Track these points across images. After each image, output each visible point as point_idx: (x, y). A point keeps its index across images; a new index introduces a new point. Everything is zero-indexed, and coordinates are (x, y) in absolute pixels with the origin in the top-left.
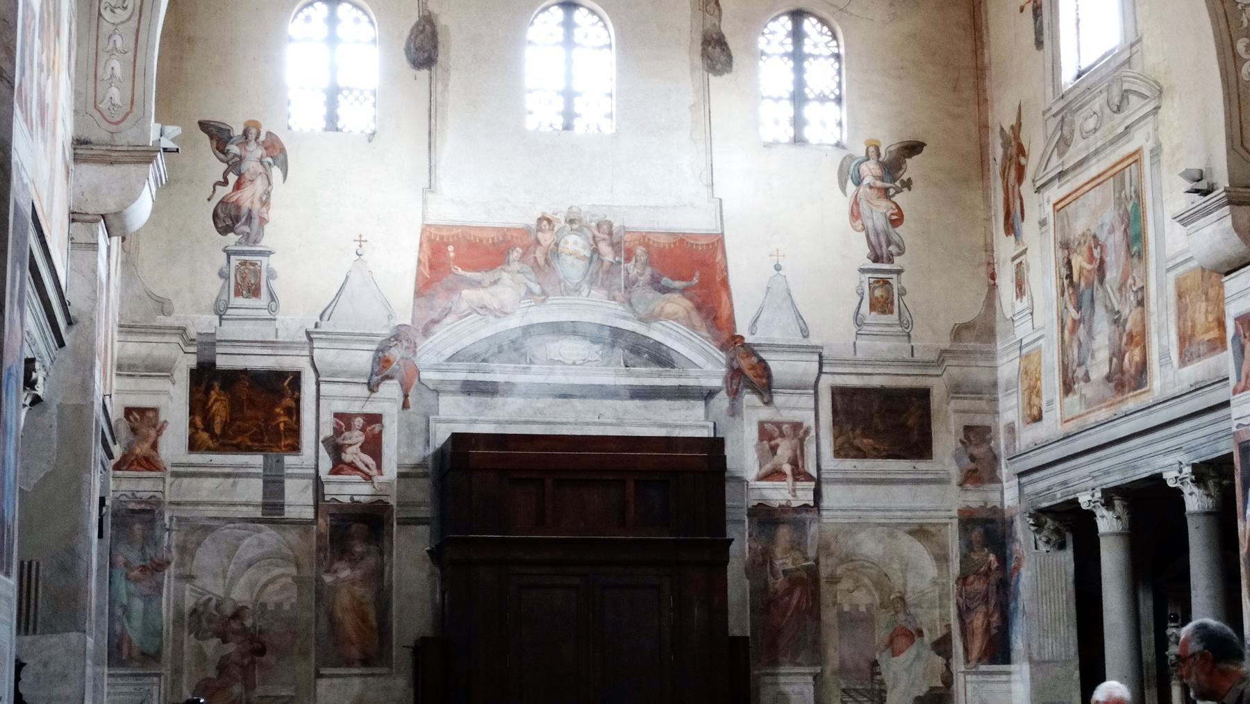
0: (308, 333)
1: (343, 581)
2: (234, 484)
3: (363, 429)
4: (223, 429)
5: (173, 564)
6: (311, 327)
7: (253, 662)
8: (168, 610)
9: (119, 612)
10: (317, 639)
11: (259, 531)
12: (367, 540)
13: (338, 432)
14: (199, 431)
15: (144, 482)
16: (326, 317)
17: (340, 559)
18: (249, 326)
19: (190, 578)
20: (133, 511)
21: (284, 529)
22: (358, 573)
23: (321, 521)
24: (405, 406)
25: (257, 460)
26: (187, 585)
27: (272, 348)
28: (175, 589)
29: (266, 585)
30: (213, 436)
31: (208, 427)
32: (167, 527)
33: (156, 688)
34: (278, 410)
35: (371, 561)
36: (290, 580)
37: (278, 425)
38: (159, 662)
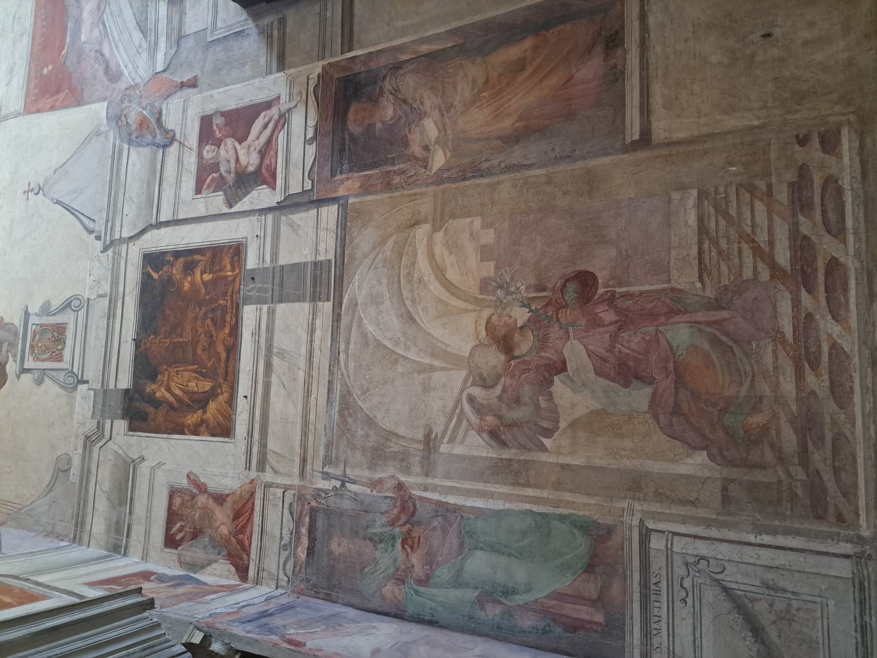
0: (105, 249)
1: (442, 129)
2: (282, 355)
3: (218, 143)
4: (204, 376)
5: (403, 478)
6: (99, 245)
7: (611, 300)
8: (492, 495)
9: (492, 612)
10: (557, 160)
11: (354, 304)
12: (374, 101)
13: (220, 185)
14: (205, 417)
15: (269, 525)
16: (91, 225)
17: (406, 143)
18: (91, 341)
19: (429, 442)
20: (311, 551)
21: (352, 257)
22: (429, 101)
23: (341, 192)
24: (193, 84)
25: (249, 314)
26: (444, 448)
27: (116, 301)
28: (448, 476)
29: (447, 285)
30: (212, 394)
31: (201, 401)
32: (338, 484)
33: (678, 545)
34: (187, 286)
35: (409, 82)
36: (439, 236)
37: (205, 283)
38: (610, 531)
